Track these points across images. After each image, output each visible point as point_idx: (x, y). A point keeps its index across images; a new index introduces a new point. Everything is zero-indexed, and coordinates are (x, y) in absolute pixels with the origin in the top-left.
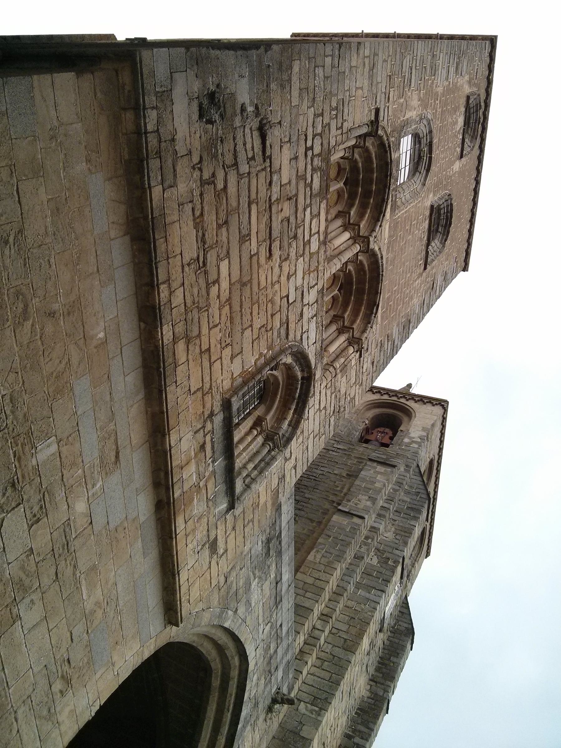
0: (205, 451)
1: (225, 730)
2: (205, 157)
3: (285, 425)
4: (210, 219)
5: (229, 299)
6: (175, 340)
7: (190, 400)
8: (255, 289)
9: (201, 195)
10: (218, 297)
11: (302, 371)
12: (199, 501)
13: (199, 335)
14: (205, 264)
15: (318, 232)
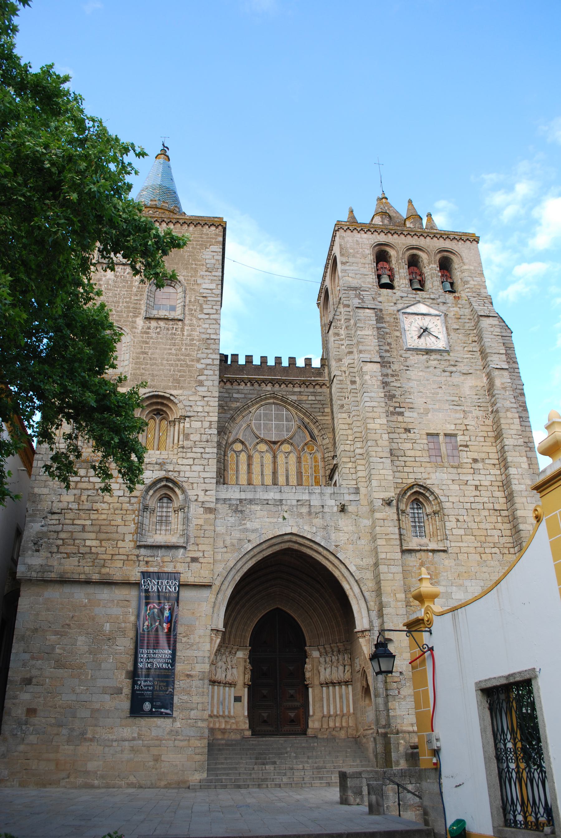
0: (149, 562)
1: (320, 549)
2: (50, 550)
3: (181, 497)
4: (70, 549)
5: (101, 541)
6: (99, 573)
7: (125, 568)
9: (61, 553)
10: (96, 547)
12: (167, 567)
13: (105, 560)
14: (82, 554)
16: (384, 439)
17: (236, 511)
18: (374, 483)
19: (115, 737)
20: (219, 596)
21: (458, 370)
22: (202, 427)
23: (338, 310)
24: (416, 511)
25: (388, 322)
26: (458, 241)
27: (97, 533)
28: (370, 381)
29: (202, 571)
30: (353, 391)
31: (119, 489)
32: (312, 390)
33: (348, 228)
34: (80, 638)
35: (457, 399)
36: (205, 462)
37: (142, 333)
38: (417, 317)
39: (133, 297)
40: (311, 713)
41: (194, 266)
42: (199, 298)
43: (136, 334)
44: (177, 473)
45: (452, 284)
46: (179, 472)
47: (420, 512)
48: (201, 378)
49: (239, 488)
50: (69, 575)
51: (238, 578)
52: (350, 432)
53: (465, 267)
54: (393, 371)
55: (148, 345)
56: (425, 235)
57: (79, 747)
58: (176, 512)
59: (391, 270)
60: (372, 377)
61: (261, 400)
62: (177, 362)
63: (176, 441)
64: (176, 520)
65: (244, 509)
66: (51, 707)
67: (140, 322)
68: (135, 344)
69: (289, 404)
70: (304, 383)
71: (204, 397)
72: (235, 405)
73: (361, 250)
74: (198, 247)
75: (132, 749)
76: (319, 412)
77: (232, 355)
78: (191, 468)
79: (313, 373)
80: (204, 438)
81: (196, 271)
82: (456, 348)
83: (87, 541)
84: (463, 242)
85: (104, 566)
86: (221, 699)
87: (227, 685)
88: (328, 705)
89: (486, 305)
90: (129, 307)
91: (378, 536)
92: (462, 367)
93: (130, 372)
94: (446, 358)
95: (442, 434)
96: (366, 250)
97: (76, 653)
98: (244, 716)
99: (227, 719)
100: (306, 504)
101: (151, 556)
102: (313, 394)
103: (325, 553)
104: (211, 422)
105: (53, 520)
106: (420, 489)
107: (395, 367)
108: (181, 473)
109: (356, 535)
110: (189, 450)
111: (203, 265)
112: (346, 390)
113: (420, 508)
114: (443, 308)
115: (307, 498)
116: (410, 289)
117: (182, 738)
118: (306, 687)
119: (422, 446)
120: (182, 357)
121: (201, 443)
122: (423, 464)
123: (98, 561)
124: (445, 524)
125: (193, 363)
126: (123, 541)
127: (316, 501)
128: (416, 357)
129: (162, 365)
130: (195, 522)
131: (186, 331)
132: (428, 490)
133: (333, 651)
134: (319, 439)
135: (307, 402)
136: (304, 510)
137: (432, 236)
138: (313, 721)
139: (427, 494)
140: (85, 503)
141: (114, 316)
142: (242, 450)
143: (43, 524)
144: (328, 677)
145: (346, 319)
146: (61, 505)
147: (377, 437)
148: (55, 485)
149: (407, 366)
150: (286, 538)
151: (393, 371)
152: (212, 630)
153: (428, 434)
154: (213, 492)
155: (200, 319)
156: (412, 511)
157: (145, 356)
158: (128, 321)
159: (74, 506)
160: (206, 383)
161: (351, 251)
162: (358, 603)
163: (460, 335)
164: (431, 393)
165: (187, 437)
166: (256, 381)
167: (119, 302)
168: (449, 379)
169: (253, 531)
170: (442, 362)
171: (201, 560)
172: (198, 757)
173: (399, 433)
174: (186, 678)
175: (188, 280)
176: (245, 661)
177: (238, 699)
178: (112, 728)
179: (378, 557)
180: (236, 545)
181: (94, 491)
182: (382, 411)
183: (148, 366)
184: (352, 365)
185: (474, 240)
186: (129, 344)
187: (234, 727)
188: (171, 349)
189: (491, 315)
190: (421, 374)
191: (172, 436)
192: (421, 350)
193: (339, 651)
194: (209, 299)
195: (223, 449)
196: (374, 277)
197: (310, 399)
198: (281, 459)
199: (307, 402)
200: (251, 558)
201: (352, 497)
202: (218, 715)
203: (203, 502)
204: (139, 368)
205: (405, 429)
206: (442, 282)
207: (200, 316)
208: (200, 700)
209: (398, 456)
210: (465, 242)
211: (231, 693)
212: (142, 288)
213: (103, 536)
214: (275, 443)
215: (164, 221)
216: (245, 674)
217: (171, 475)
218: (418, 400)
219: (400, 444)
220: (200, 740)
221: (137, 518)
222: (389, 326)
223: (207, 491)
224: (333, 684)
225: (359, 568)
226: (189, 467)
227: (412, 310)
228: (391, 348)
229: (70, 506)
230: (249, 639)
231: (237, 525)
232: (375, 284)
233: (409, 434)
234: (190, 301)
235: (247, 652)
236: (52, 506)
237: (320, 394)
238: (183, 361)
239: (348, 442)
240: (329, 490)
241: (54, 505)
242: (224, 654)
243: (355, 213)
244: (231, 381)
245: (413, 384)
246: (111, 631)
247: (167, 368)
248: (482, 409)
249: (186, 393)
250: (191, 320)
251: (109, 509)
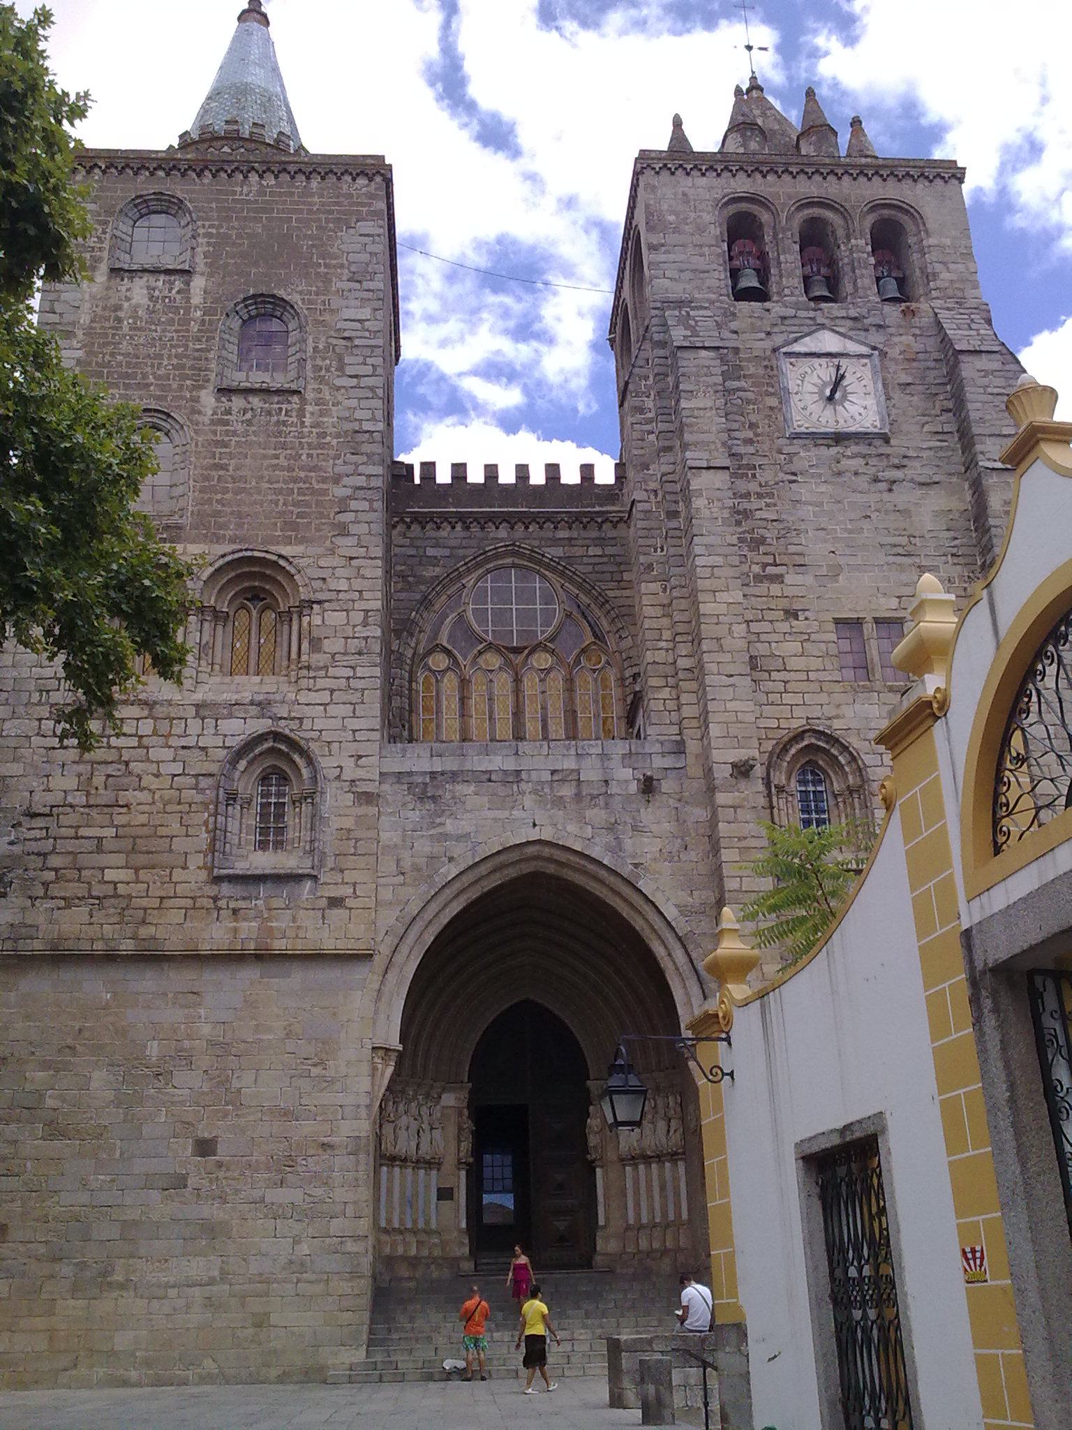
0: (240, 909)
2: (29, 893)
3: (305, 772)
5: (137, 870)
7: (188, 924)
8: (145, 831)
9: (52, 898)
10: (128, 883)
11: (266, 740)
13: (145, 909)
14: (98, 898)
15: (138, 719)
16: (735, 635)
17: (422, 799)
18: (714, 730)
19: (172, 1279)
20: (389, 976)
21: (909, 477)
22: (348, 623)
23: (642, 354)
24: (811, 788)
25: (751, 376)
26: (915, 181)
27: (128, 853)
28: (707, 512)
30: (671, 533)
31: (174, 761)
32: (594, 534)
33: (665, 165)
34: (96, 1075)
35: (904, 541)
36: (355, 697)
37: (213, 422)
38: (816, 361)
39: (191, 344)
40: (601, 1222)
41: (322, 269)
42: (334, 342)
43: (201, 426)
44: (297, 722)
45: (902, 282)
46: (301, 719)
47: (819, 789)
48: (343, 518)
49: (428, 751)
50: (70, 944)
51: (429, 939)
52: (665, 622)
53: (932, 241)
54: (761, 485)
55: (228, 450)
56: (840, 171)
57: (97, 1302)
58: (297, 804)
59: (762, 256)
60: (710, 501)
61: (487, 560)
62: (291, 486)
63: (294, 655)
64: (297, 820)
65: (440, 792)
66: (37, 1220)
67: (208, 399)
68: (200, 449)
69: (548, 567)
70: (577, 518)
71: (351, 558)
72: (429, 572)
73: (693, 215)
74: (331, 225)
75: (209, 1302)
76: (612, 581)
77: (423, 464)
78: (325, 709)
79: (597, 496)
80: (354, 645)
81: (327, 280)
82: (905, 427)
83: (106, 870)
84: (927, 183)
85: (144, 922)
86: (409, 1193)
87: (421, 1165)
88: (637, 1205)
89: (974, 326)
90: (183, 367)
91: (723, 843)
92: (916, 470)
93: (190, 509)
94: (881, 451)
95: (869, 619)
96: (704, 215)
97: (89, 1106)
98: (460, 1231)
99: (423, 1237)
100: (570, 778)
101: (244, 899)
102: (597, 542)
103: (612, 879)
104: (368, 611)
105: (34, 829)
106: (819, 740)
107: (766, 476)
108: (305, 721)
109: (679, 840)
110: (322, 673)
111: (342, 266)
112: (658, 531)
113: (820, 782)
114: (876, 338)
115: (573, 766)
116: (805, 298)
117: (313, 1277)
119: (823, 646)
120: (302, 474)
121: (346, 658)
122: (826, 686)
123: (131, 912)
124: (873, 813)
125: (325, 486)
126: (185, 868)
127: (591, 773)
128: (814, 452)
129: (259, 493)
130: (336, 823)
131: (308, 415)
132: (837, 740)
134: (611, 642)
135: (585, 560)
136: (567, 791)
137: (855, 172)
139: (834, 751)
140: (101, 791)
141: (152, 388)
142: (448, 669)
143: (13, 838)
145: (656, 375)
146: (51, 799)
147: (721, 631)
148: (35, 757)
149: (794, 474)
150: (531, 850)
151: (761, 485)
152: (373, 1048)
153: (837, 621)
154: (374, 760)
155: (338, 389)
156: (803, 789)
157: (222, 473)
158: (182, 398)
159: (80, 799)
160: (354, 529)
161: (672, 218)
162: (685, 987)
163: (915, 398)
164: (846, 530)
165: (316, 645)
166: (475, 520)
167: (161, 357)
168: (886, 496)
169: (459, 838)
170: (873, 461)
171: (349, 903)
173: (771, 622)
174: (320, 1151)
175: (310, 302)
176: (460, 1115)
177: (445, 1194)
178: (166, 1261)
179: (723, 886)
181: (119, 766)
182: (731, 574)
183: (228, 496)
184: (670, 478)
185: (954, 176)
186: (184, 449)
187: (437, 1252)
188: (277, 457)
189: (983, 348)
190: (823, 488)
191: (285, 645)
192: (825, 436)
194: (357, 342)
195: (407, 668)
196: (723, 277)
197: (590, 553)
198: (531, 684)
199: (585, 560)
201: (669, 762)
203: (354, 781)
204: (210, 499)
205: (786, 612)
206: (878, 279)
207: (338, 382)
209: (769, 672)
210: (931, 181)
211: (433, 1179)
212: (211, 323)
213: (141, 859)
214: (517, 651)
215: (253, 168)
216: (459, 1141)
217: (284, 728)
218: (815, 548)
219: (774, 645)
220: (349, 1280)
221: (212, 819)
222: (754, 384)
223: (360, 757)
224: (647, 1159)
225: (683, 909)
226: (322, 708)
227: (806, 345)
228: (757, 435)
229: (70, 799)
231: (425, 826)
232: (724, 291)
233: (795, 623)
234: (315, 348)
235: (464, 1095)
236: (31, 801)
237: (613, 542)
238: (304, 483)
239: (663, 644)
240: (619, 748)
241: (36, 797)
242: (414, 1098)
243: (686, 128)
244: (421, 520)
245: (807, 511)
246: (162, 1058)
247: (270, 498)
248: (961, 560)
249: (312, 550)
250: (320, 391)
251: (154, 803)
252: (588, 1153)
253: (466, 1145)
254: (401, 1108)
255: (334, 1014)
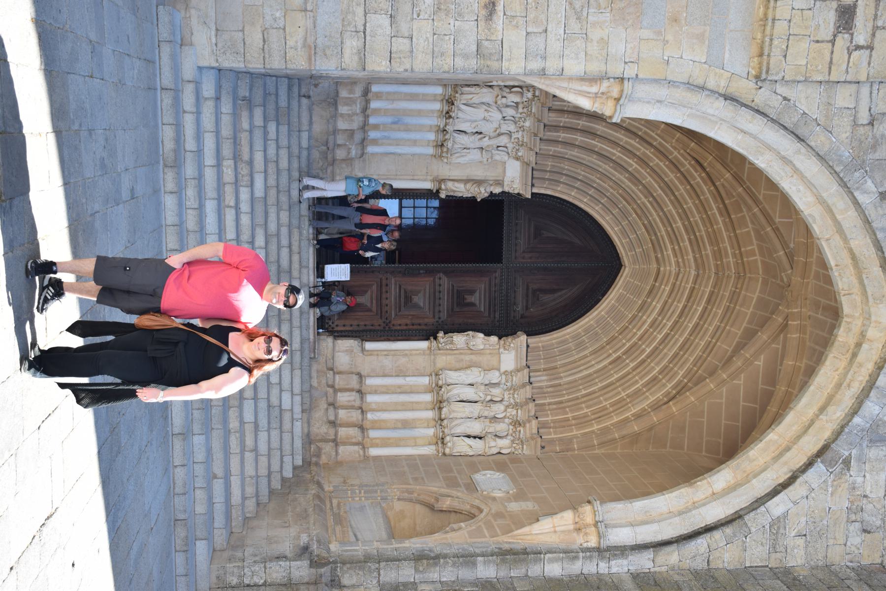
1: (837, 413)
29: (804, 45)
40: (369, 346)
51: (761, 161)
88: (387, 390)
99: (358, 137)
109: (879, 523)
118: (429, 334)
133: (516, 406)
138: (350, 351)
144: (455, 392)
171: (842, 41)
172: (255, 38)
180: (877, 156)
193: (516, 423)
200: (822, 202)
202: (369, 112)
208: (421, 43)
216: (466, 181)
224: (439, 404)
225: (778, 524)
230: (549, 192)
252: (445, 333)
253: (462, 191)
254: (510, 112)
255: (676, 21)
